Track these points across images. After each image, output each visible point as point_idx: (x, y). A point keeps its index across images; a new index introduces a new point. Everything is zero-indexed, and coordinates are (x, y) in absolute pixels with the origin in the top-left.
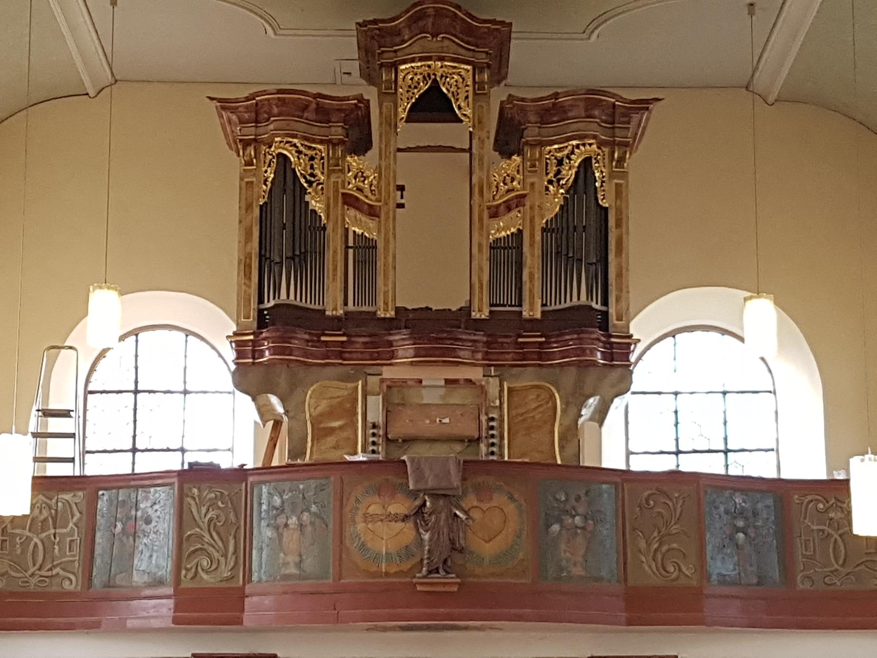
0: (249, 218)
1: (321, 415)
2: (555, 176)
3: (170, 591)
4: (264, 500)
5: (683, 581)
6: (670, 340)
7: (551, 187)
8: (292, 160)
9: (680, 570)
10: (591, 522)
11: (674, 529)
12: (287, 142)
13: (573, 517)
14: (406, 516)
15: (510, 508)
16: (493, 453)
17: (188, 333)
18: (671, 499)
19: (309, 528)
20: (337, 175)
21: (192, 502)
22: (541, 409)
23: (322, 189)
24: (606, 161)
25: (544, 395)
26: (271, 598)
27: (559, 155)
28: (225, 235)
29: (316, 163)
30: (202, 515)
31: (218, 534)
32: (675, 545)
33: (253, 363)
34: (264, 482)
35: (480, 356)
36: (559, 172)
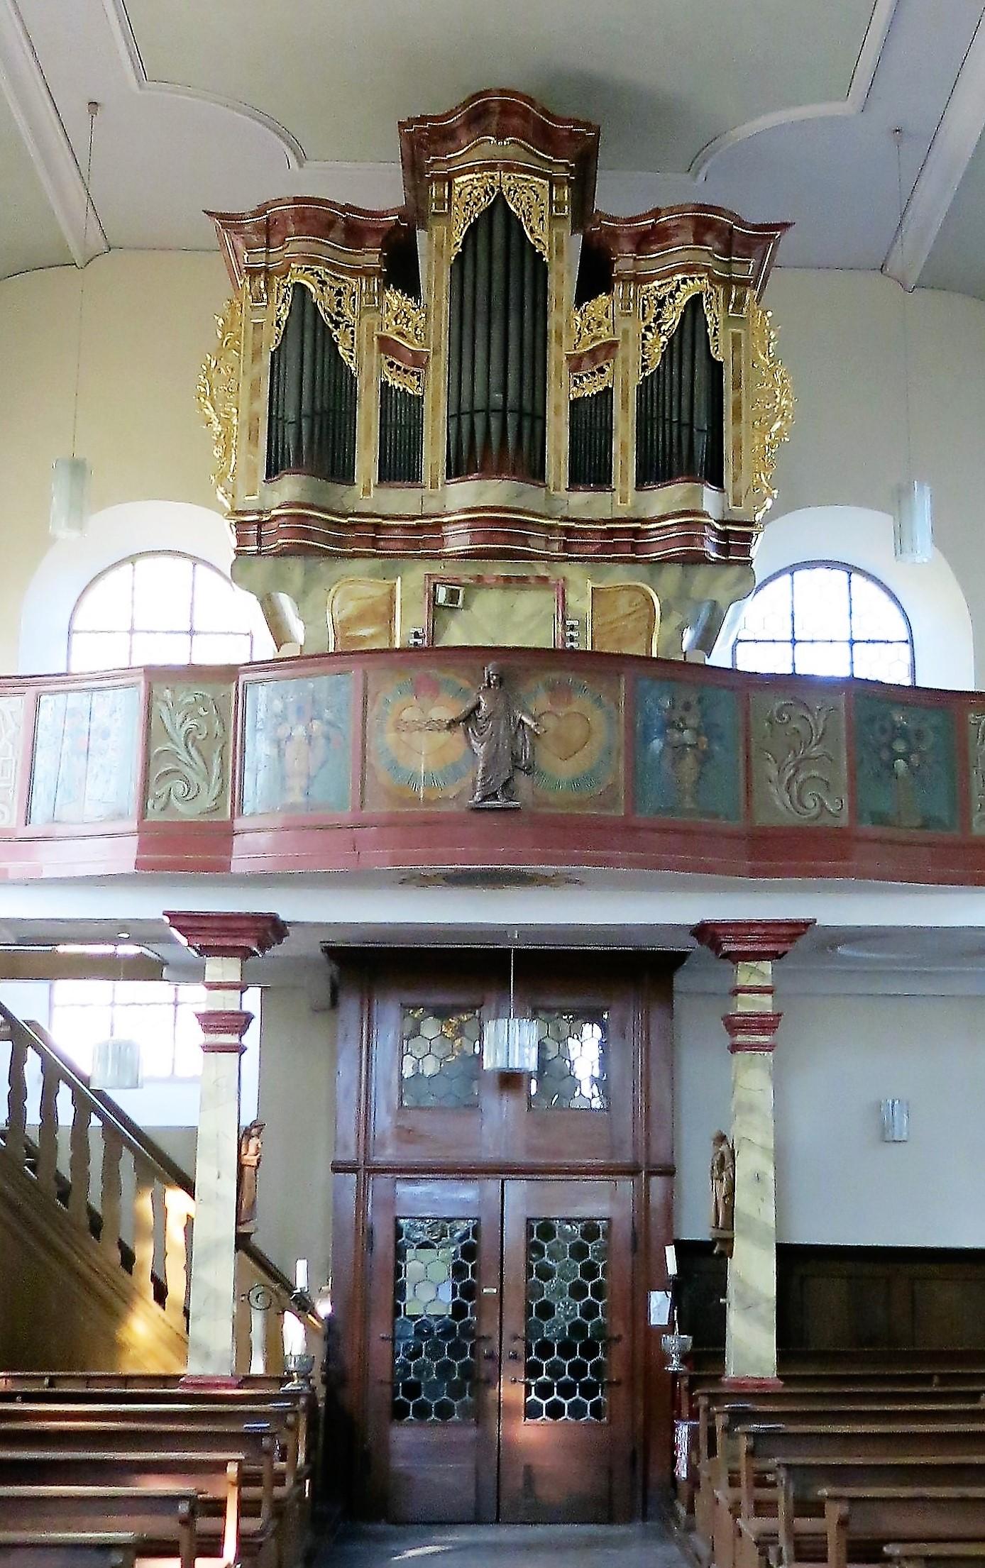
0: (257, 368)
1: (348, 620)
2: (655, 320)
3: (133, 826)
4: (262, 707)
5: (827, 821)
6: (786, 578)
7: (649, 335)
8: (313, 290)
9: (823, 805)
10: (704, 739)
11: (815, 751)
12: (307, 269)
13: (682, 730)
14: (453, 721)
15: (597, 717)
16: (572, 639)
17: (196, 560)
18: (809, 710)
19: (322, 741)
20: (372, 315)
21: (164, 709)
22: (634, 616)
23: (352, 332)
24: (721, 305)
25: (640, 598)
26: (269, 835)
27: (660, 294)
28: (229, 408)
29: (345, 300)
30: (175, 724)
31: (199, 751)
32: (815, 773)
33: (259, 553)
34: (261, 682)
35: (556, 546)
36: (659, 316)
